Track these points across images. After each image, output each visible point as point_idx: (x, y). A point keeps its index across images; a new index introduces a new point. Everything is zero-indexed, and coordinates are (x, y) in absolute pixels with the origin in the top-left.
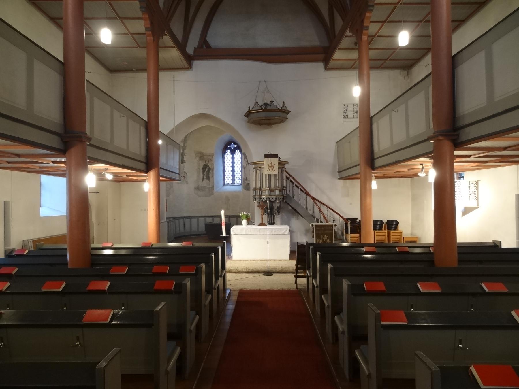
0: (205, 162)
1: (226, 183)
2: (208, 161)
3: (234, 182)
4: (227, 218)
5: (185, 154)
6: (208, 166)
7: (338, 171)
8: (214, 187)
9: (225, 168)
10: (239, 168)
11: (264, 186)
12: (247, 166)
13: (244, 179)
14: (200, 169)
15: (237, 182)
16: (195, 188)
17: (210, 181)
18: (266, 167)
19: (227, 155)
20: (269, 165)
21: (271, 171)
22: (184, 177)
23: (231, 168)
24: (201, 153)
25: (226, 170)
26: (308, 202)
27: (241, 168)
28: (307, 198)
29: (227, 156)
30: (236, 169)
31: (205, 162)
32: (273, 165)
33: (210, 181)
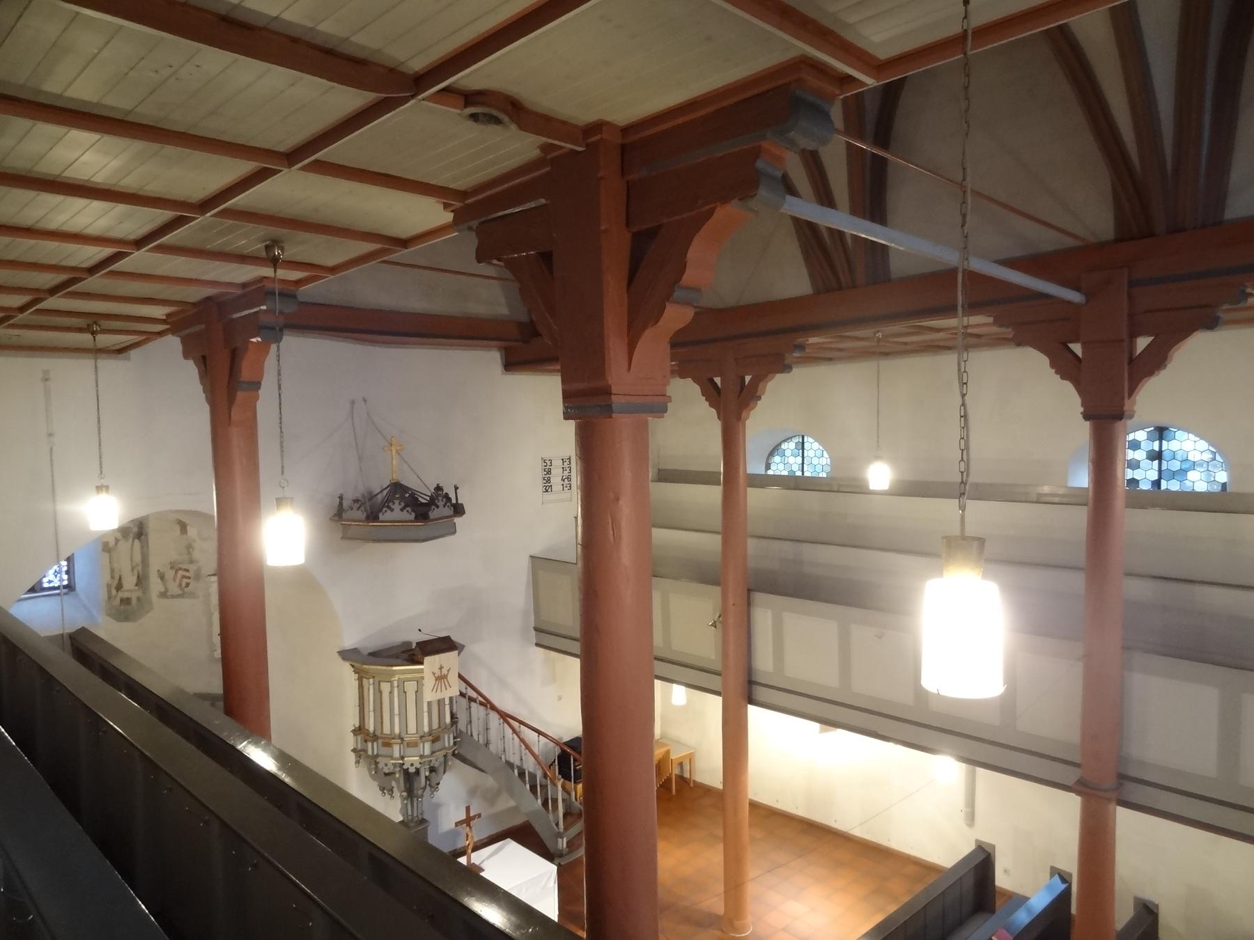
7: (533, 625)
11: (412, 728)
13: (109, 586)
15: (50, 582)
18: (429, 682)
20: (436, 675)
21: (441, 691)
26: (472, 720)
28: (472, 709)
32: (444, 671)
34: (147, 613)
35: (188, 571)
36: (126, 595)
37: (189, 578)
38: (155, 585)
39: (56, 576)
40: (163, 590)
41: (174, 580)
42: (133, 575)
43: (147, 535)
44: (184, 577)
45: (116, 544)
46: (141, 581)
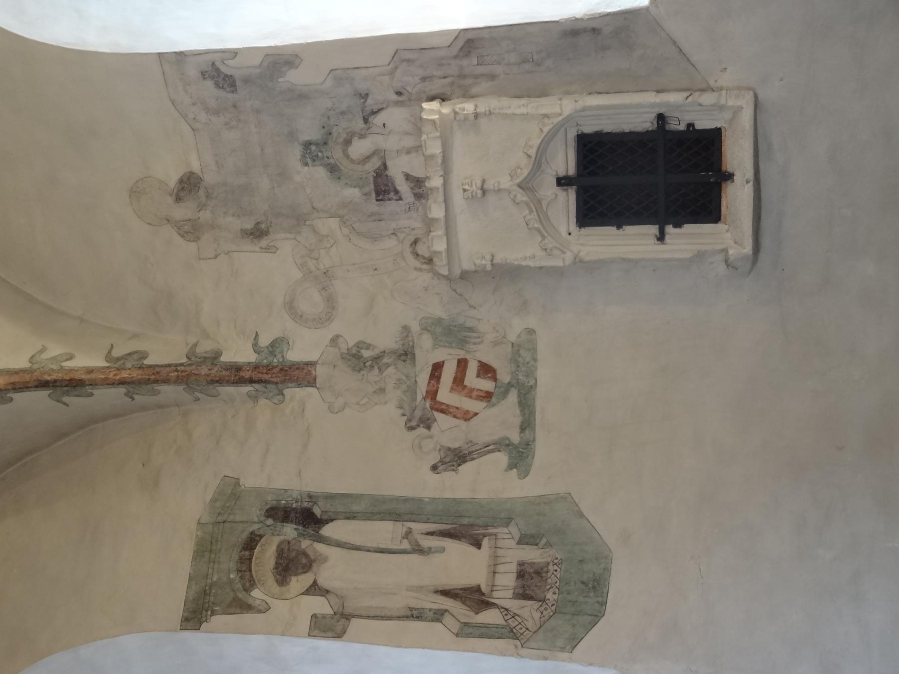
12: (326, 576)
13: (467, 631)
34: (581, 515)
35: (437, 368)
36: (507, 580)
37: (462, 364)
40: (502, 458)
41: (468, 416)
42: (442, 550)
43: (310, 496)
45: (325, 592)
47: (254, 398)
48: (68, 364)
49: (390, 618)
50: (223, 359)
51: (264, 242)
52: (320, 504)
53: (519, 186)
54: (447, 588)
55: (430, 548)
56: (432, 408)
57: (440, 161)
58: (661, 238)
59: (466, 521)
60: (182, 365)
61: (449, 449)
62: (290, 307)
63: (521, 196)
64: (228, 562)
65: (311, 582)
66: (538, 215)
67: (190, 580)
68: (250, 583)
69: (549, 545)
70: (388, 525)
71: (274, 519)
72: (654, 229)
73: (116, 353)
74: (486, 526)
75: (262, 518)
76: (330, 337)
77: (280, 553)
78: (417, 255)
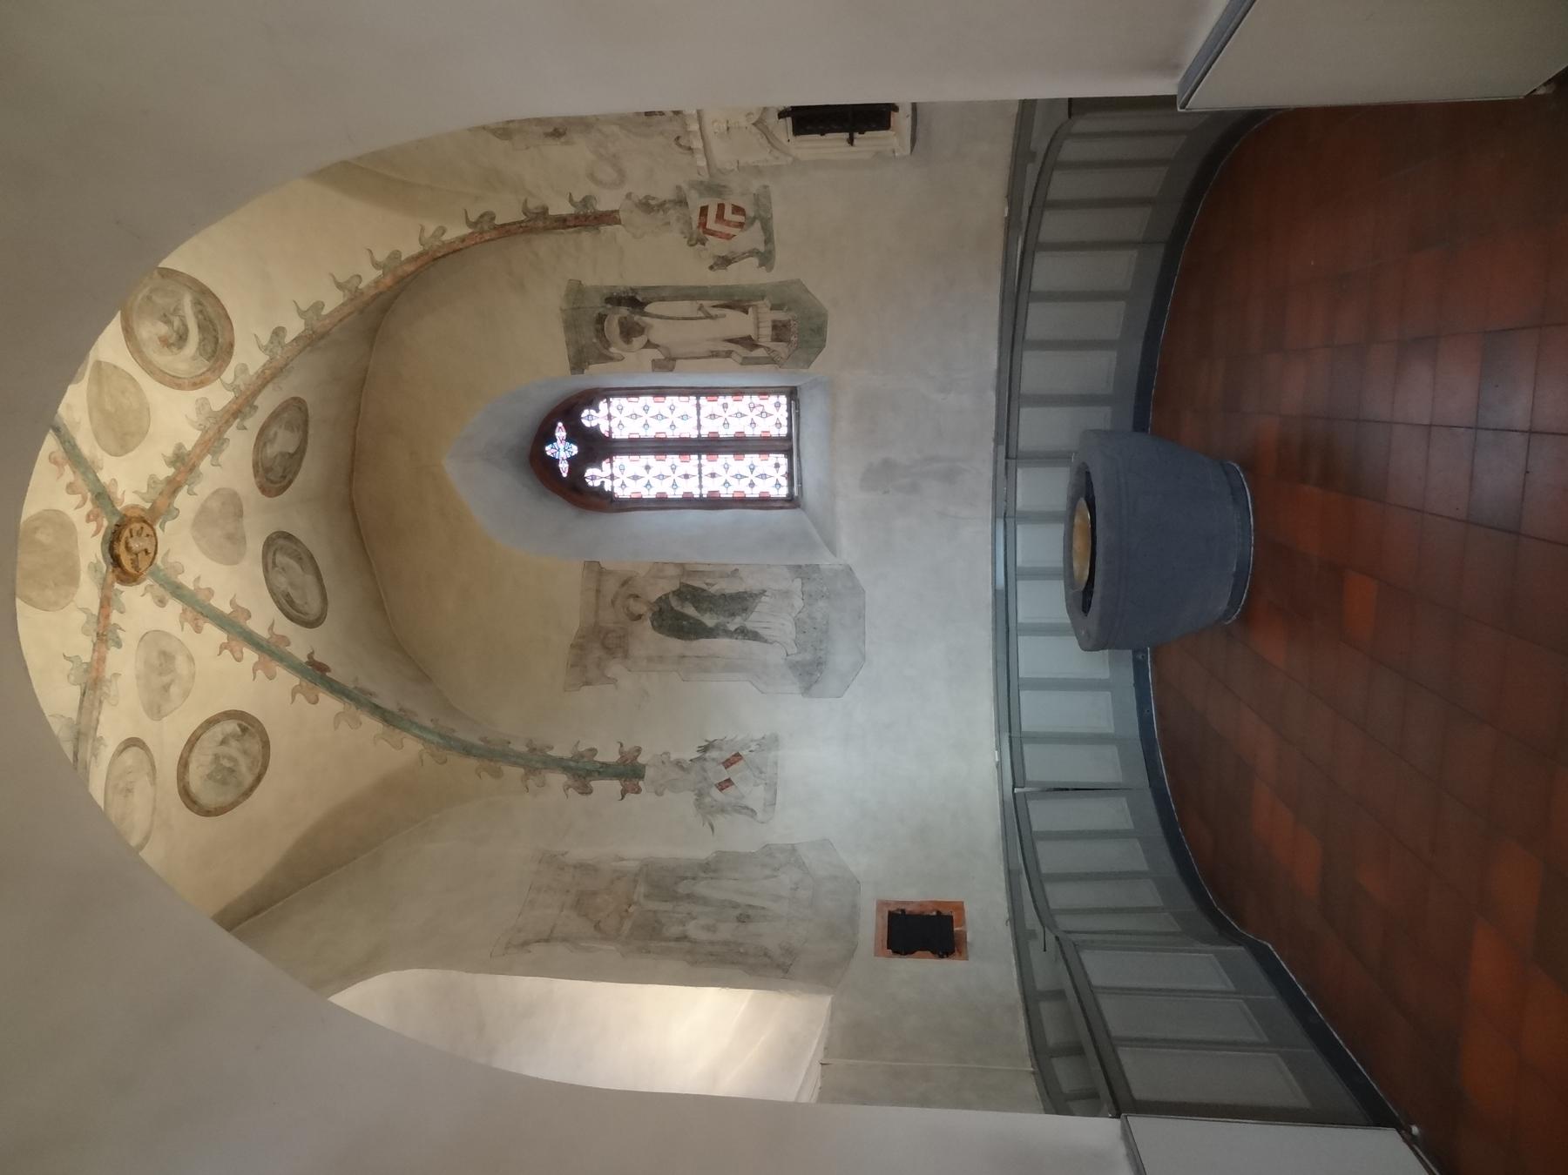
0: (639, 617)
1: (783, 492)
2: (631, 601)
3: (779, 439)
4: (1020, 471)
5: (582, 756)
6: (664, 599)
8: (800, 567)
9: (697, 496)
10: (693, 411)
12: (655, 339)
13: (746, 361)
14: (684, 657)
15: (778, 425)
16: (807, 690)
17: (763, 592)
19: (617, 483)
22: (728, 763)
23: (694, 457)
24: (580, 647)
25: (710, 486)
27: (693, 399)
29: (623, 484)
30: (699, 426)
31: (639, 617)
33: (763, 592)
34: (807, 291)
36: (766, 331)
37: (721, 207)
38: (744, 274)
39: (768, 415)
40: (755, 261)
41: (729, 237)
42: (724, 316)
43: (632, 289)
44: (720, 216)
45: (656, 346)
46: (736, 301)
47: (579, 232)
48: (446, 237)
49: (698, 358)
50: (551, 212)
51: (563, 139)
52: (640, 292)
53: (754, 124)
54: (731, 338)
55: (717, 316)
56: (704, 232)
57: (696, 117)
58: (851, 141)
59: (736, 298)
60: (522, 221)
61: (719, 257)
62: (592, 176)
63: (754, 129)
64: (588, 336)
65: (645, 342)
66: (767, 139)
67: (567, 345)
68: (607, 344)
69: (789, 309)
70: (687, 303)
71: (611, 304)
72: (846, 135)
73: (473, 217)
74: (749, 301)
75: (604, 304)
76: (625, 193)
77: (621, 324)
78: (680, 146)
